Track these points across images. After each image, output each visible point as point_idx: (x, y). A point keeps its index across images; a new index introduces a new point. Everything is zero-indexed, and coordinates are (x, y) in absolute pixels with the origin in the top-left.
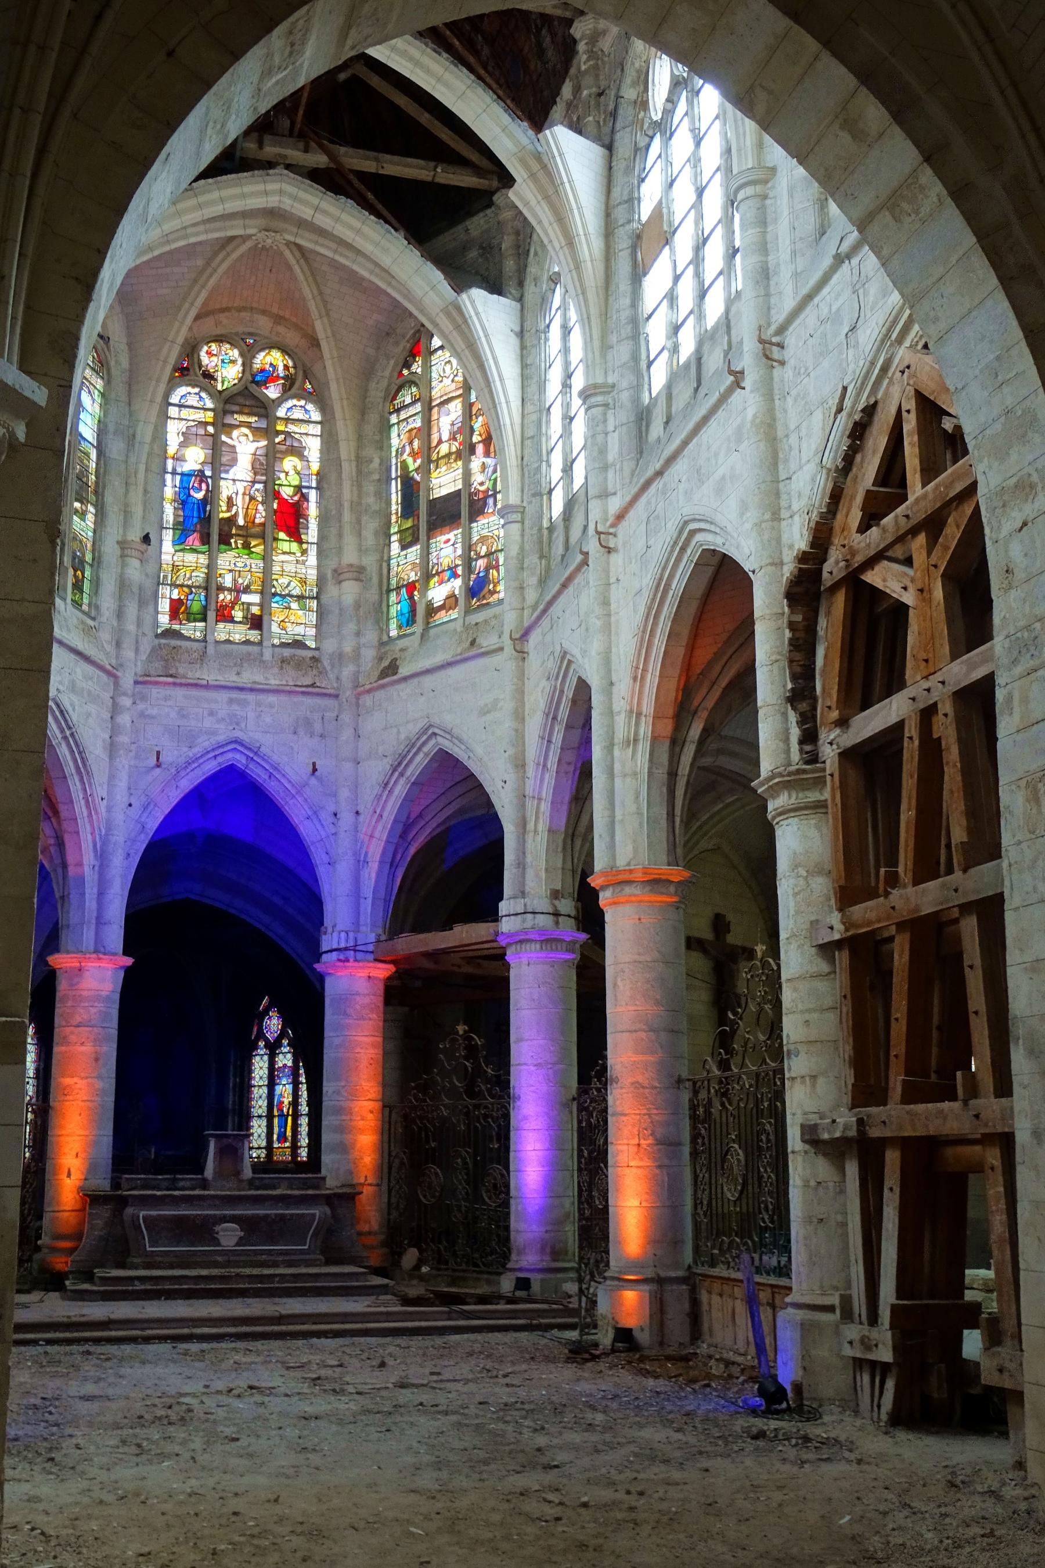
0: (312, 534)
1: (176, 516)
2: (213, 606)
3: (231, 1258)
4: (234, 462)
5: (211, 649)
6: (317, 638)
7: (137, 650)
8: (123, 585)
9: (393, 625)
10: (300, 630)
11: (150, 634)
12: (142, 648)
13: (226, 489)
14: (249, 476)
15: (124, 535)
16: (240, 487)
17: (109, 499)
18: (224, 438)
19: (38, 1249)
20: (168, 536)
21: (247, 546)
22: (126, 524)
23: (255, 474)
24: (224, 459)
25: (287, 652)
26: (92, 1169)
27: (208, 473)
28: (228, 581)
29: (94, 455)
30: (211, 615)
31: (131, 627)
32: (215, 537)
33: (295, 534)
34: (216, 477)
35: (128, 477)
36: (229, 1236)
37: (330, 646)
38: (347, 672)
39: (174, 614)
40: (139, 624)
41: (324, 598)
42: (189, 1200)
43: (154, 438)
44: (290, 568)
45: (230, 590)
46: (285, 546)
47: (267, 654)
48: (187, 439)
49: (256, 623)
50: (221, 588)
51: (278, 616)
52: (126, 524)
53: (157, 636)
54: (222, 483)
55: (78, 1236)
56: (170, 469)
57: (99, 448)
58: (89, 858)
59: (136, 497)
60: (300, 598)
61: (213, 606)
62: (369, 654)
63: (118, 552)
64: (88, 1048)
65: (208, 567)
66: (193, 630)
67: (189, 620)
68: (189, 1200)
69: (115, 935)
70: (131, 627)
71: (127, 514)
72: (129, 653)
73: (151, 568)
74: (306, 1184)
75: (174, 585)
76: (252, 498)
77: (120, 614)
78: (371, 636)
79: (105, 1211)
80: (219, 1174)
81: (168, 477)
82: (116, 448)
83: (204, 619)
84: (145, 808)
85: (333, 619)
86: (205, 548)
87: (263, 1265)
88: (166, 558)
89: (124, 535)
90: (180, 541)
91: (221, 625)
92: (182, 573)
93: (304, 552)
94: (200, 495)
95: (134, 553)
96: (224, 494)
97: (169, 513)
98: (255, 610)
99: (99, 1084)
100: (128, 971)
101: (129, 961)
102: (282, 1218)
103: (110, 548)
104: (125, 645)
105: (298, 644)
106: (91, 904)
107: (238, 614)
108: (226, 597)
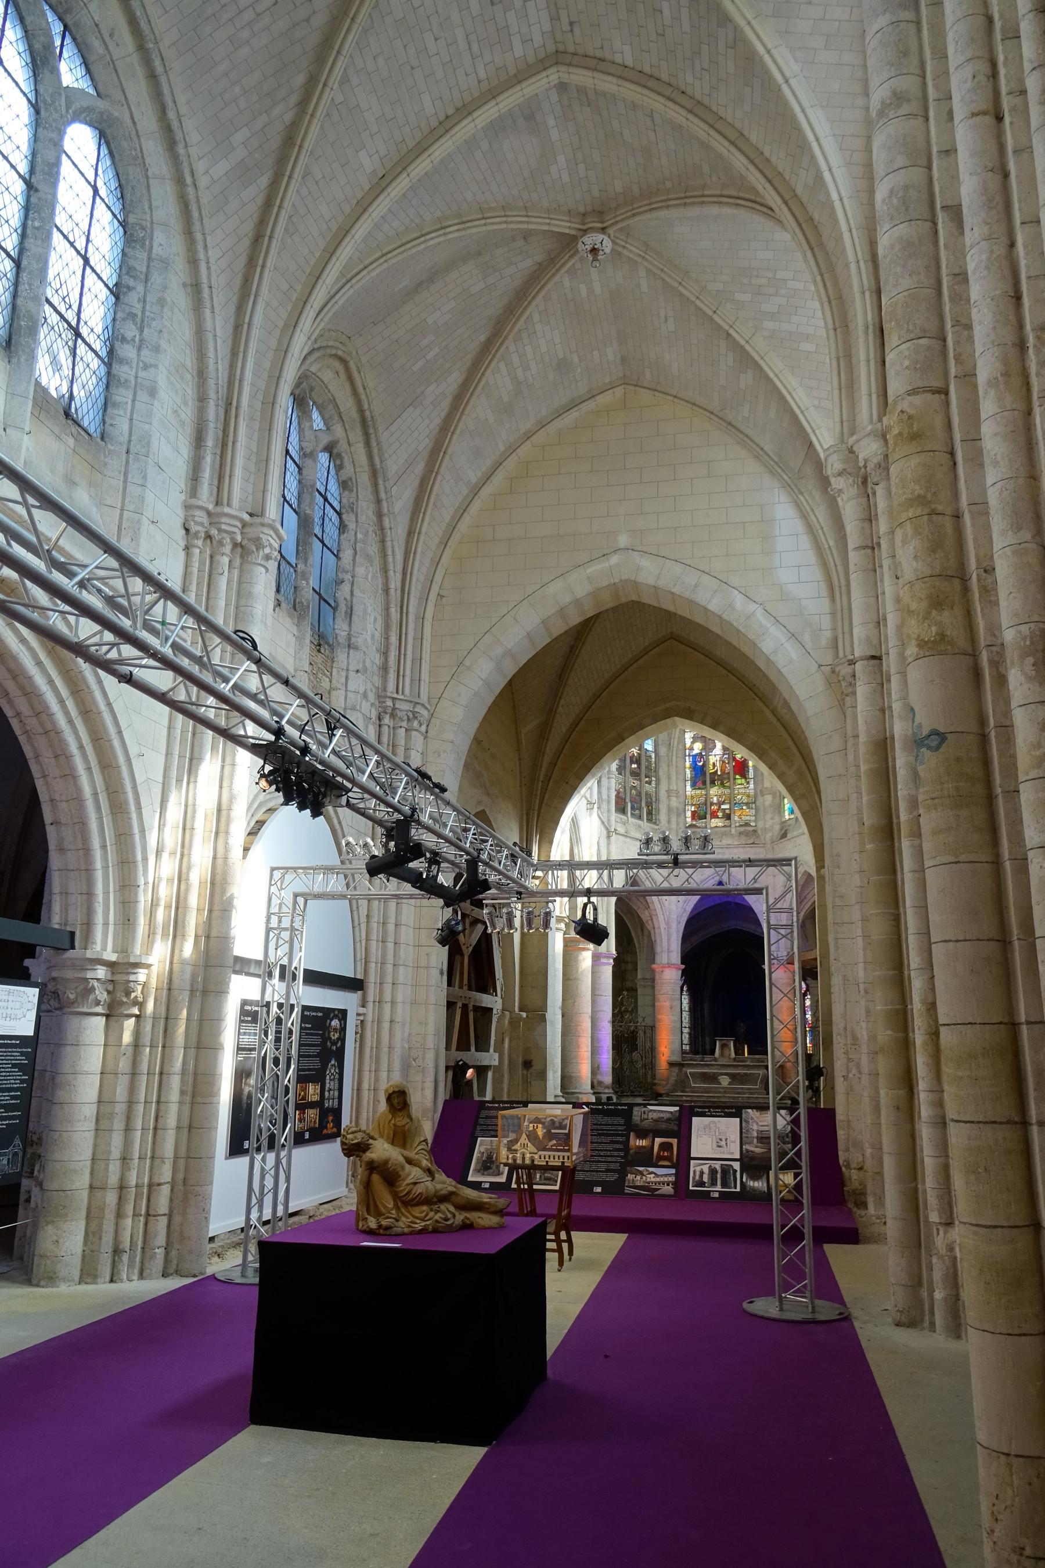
0: (751, 774)
2: (709, 812)
3: (726, 1090)
6: (755, 821)
8: (669, 809)
9: (787, 813)
10: (748, 818)
13: (712, 759)
16: (718, 758)
17: (661, 773)
19: (655, 1084)
20: (688, 784)
21: (722, 784)
22: (669, 783)
25: (742, 829)
26: (673, 1052)
28: (715, 800)
29: (653, 756)
30: (708, 816)
32: (708, 782)
33: (744, 776)
34: (708, 755)
36: (725, 1081)
37: (760, 825)
38: (769, 835)
40: (678, 824)
41: (758, 803)
42: (708, 1065)
43: (678, 744)
44: (741, 791)
46: (739, 781)
47: (733, 831)
48: (695, 739)
49: (728, 817)
50: (712, 804)
51: (738, 813)
52: (669, 783)
55: (668, 1079)
57: (656, 751)
58: (663, 925)
60: (747, 804)
61: (709, 812)
62: (777, 827)
64: (667, 1004)
66: (700, 823)
68: (708, 1065)
69: (676, 957)
71: (669, 778)
73: (682, 799)
74: (758, 1060)
75: (692, 805)
77: (669, 822)
78: (777, 819)
79: (676, 1070)
80: (722, 1054)
82: (663, 751)
85: (761, 812)
87: (739, 1093)
90: (694, 786)
93: (748, 783)
96: (711, 762)
97: (688, 772)
98: (727, 811)
99: (672, 1018)
100: (683, 971)
101: (683, 967)
102: (746, 1074)
103: (663, 794)
105: (747, 824)
106: (665, 944)
107: (720, 814)
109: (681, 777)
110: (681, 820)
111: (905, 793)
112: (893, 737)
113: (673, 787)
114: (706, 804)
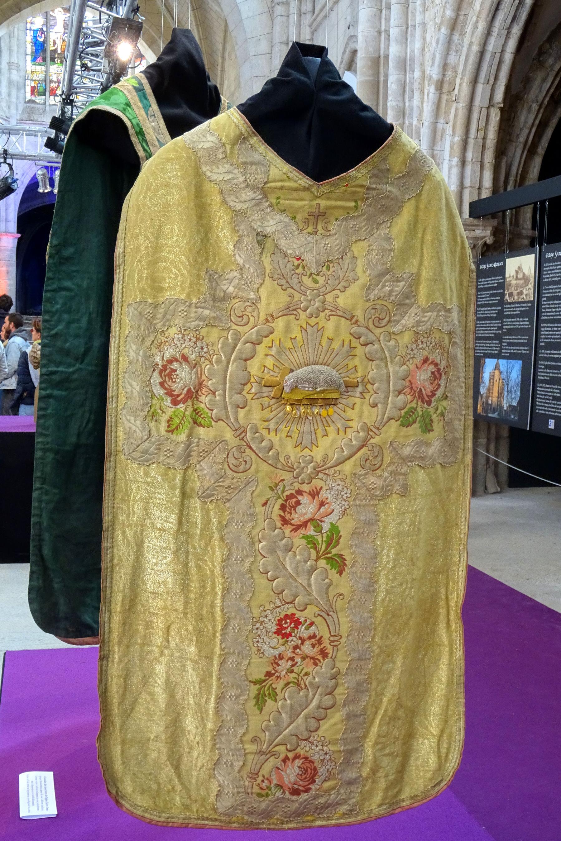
1: (32, 49)
4: (56, 23)
5: (47, 108)
7: (17, 109)
8: (10, 82)
11: (23, 102)
12: (19, 109)
13: (53, 36)
14: (62, 30)
15: (10, 60)
16: (59, 35)
18: (51, 13)
20: (29, 58)
23: (65, 29)
24: (52, 23)
27: (45, 29)
28: (54, 78)
30: (48, 93)
31: (14, 100)
32: (48, 59)
35: (10, 34)
39: (32, 93)
40: (18, 98)
45: (55, 82)
50: (51, 81)
53: (25, 102)
54: (51, 34)
56: (28, 28)
59: (14, 43)
61: (48, 89)
63: (7, 67)
65: (46, 72)
67: (39, 95)
70: (14, 100)
71: (11, 51)
72: (13, 111)
73: (22, 73)
75: (32, 80)
76: (64, 41)
77: (9, 95)
81: (28, 31)
83: (45, 95)
84: (23, 175)
86: (44, 63)
88: (29, 69)
89: (10, 60)
90: (34, 60)
91: (52, 97)
92: (35, 75)
94: (41, 40)
95: (14, 67)
104: (12, 108)
108: (54, 85)
109: (22, 51)
110: (21, 96)
111: (395, 104)
112: (387, 57)
113: (14, 60)
114: (45, 81)
